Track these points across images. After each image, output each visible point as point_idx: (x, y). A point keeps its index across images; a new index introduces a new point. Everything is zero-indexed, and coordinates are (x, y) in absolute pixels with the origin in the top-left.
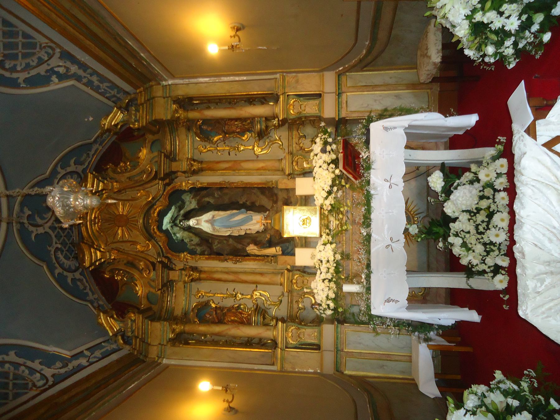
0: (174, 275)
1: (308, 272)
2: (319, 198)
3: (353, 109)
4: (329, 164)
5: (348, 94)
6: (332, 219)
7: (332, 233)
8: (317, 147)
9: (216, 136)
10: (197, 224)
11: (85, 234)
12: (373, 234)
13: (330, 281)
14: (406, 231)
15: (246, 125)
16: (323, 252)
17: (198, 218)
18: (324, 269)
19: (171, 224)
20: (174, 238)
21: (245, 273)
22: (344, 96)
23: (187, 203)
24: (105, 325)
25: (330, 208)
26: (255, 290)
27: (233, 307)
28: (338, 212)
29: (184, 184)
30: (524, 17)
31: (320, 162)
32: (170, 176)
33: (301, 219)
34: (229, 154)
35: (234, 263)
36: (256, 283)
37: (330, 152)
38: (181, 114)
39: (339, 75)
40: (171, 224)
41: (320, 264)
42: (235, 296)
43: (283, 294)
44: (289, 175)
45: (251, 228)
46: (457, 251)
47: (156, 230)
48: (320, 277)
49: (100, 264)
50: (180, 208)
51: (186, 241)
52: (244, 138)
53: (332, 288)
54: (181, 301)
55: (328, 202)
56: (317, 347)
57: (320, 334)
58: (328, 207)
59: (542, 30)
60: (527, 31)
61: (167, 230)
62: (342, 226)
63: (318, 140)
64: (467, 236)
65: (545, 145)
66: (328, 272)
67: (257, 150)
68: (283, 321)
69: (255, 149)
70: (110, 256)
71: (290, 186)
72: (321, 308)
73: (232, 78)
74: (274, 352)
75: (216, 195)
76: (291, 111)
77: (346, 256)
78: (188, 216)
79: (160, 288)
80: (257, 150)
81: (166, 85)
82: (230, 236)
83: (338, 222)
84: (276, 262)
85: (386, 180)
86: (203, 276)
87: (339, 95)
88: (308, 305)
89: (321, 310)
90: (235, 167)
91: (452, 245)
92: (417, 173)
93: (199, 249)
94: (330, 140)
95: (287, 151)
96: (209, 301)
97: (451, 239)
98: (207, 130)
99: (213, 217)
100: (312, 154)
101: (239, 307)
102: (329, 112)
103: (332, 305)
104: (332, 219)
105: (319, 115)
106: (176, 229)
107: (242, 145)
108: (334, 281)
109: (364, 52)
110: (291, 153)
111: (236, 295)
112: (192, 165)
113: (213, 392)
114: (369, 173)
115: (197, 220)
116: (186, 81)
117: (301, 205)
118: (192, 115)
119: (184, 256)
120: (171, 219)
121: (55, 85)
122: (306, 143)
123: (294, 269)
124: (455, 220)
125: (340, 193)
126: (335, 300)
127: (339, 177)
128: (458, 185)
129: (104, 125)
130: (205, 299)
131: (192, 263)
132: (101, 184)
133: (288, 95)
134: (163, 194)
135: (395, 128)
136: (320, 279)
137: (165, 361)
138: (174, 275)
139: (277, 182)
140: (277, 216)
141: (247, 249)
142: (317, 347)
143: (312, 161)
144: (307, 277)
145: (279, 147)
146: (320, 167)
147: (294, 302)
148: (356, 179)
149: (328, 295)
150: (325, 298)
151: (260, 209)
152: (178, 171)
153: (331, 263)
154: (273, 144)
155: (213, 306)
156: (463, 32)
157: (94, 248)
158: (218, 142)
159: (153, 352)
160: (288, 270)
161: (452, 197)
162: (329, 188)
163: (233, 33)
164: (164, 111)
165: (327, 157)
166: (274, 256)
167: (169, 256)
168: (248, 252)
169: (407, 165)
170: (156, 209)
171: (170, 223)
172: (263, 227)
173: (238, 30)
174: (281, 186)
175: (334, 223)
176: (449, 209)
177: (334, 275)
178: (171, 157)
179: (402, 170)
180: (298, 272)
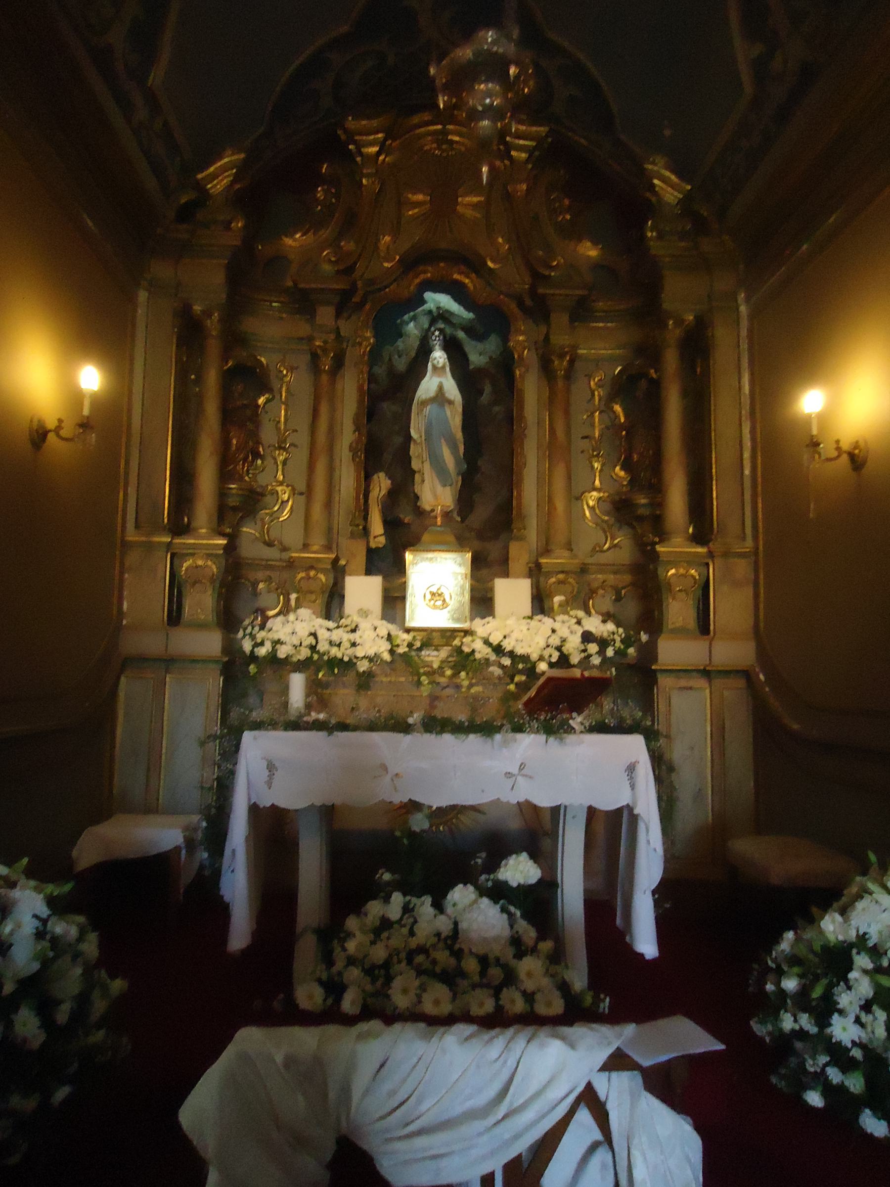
0: (325, 315)
1: (332, 603)
2: (483, 628)
3: (674, 701)
4: (559, 649)
5: (708, 691)
6: (444, 653)
7: (413, 653)
8: (594, 624)
9: (624, 410)
10: (435, 368)
11: (416, 120)
12: (409, 738)
13: (313, 648)
14: (414, 806)
15: (646, 475)
16: (373, 634)
17: (448, 369)
18: (336, 635)
19: (434, 310)
20: (406, 317)
21: (331, 469)
22: (702, 683)
23: (480, 346)
24: (219, 164)
25: (466, 649)
26: (293, 489)
27: (258, 443)
28: (458, 667)
29: (521, 338)
30: (857, 1053)
31: (563, 631)
32: (539, 309)
33: (442, 590)
34: (583, 438)
35: (350, 446)
36: (308, 493)
37: (585, 651)
38: (673, 333)
39: (746, 674)
40: (434, 310)
41: (349, 629)
42: (280, 448)
43: (285, 549)
44: (538, 566)
45: (426, 482)
46: (375, 908)
47: (422, 277)
48: (321, 626)
49: (350, 156)
50: (469, 330)
51: (400, 344)
52: (618, 468)
53: (299, 652)
54: (272, 332)
55: (478, 645)
56: (175, 618)
57: (202, 626)
58: (469, 646)
59: (830, 1091)
60: (828, 1059)
61: (423, 302)
62: (425, 674)
63: (610, 626)
64: (405, 931)
65: (589, 1087)
66: (331, 643)
67: (592, 497)
68: (231, 548)
69: (595, 494)
70: (368, 176)
71: (513, 565)
72: (257, 628)
73: (747, 443)
74: (164, 528)
75: (496, 409)
76: (673, 571)
77: (365, 681)
78: (452, 347)
79: (302, 286)
80: (592, 497)
81: (736, 301)
82: (409, 438)
83: (435, 666)
84: (353, 536)
85: (522, 766)
86: (325, 378)
87: (706, 673)
88: (262, 602)
89: (253, 628)
90: (556, 450)
91: (387, 900)
92: (536, 831)
93: (380, 371)
94: (610, 652)
95: (590, 560)
96: (270, 390)
97: (397, 898)
98: (637, 390)
99: (451, 402)
100: (581, 614)
101: (257, 455)
102: (673, 651)
103: (262, 651)
104: (444, 653)
105: (665, 629)
106: (425, 322)
107: (603, 465)
108: (312, 657)
109: (795, 726)
110: (584, 570)
111: (284, 449)
112: (562, 356)
113: (75, 396)
114: (537, 732)
115: (443, 367)
116: (744, 345)
117: (473, 589)
118: (671, 359)
119: (367, 339)
120: (447, 311)
121: (743, 52)
122: (606, 601)
123: (339, 573)
124: (439, 906)
125: (496, 671)
126: (272, 659)
127: (531, 672)
128: (511, 915)
129: (654, 163)
130: (276, 384)
131: (352, 355)
132: (524, 155)
133: (707, 565)
134: (501, 293)
135: (633, 787)
136: (317, 627)
137: (143, 296)
138: (325, 315)
139: (521, 539)
140: (451, 538)
141: (382, 475)
142: (175, 618)
143: (567, 613)
144: (320, 602)
145: (598, 545)
146: (554, 631)
147: (268, 573)
148: (526, 704)
149: (282, 643)
150: (276, 637)
151: (466, 500)
152: (549, 326)
153: (350, 651)
154: (605, 532)
155: (261, 401)
156: (831, 928)
157: (385, 139)
158: (611, 415)
159: (162, 270)
160: (336, 560)
161: (485, 901)
162: (508, 649)
163: (845, 445)
164: (681, 296)
165: (574, 644)
167: (367, 307)
168: (375, 477)
169: (555, 811)
170: (468, 277)
171: (438, 308)
172: (428, 508)
173: (852, 456)
174: (515, 549)
175: (434, 657)
176: (461, 895)
177: (326, 658)
178: (581, 312)
179: (544, 801)
180: (332, 581)
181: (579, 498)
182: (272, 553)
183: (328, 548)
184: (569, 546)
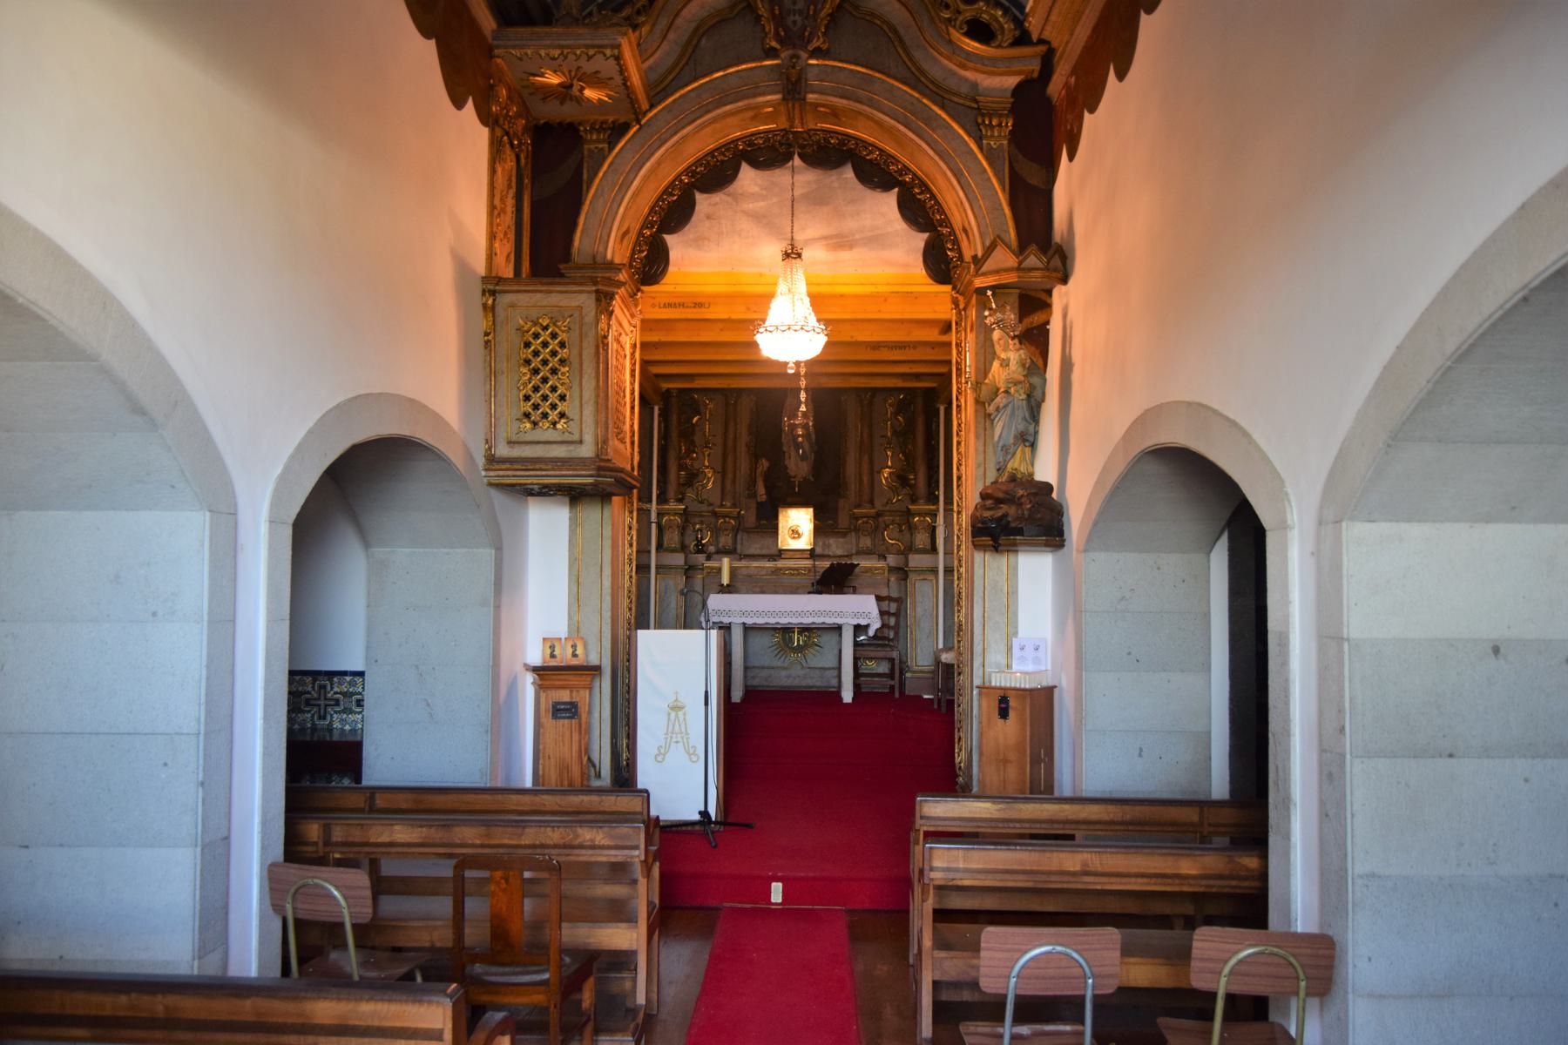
57: (674, 551)
84: (749, 496)
110: (879, 514)
166: (755, 495)
181: (879, 472)
182: (704, 507)
183: (734, 506)
184: (872, 502)
